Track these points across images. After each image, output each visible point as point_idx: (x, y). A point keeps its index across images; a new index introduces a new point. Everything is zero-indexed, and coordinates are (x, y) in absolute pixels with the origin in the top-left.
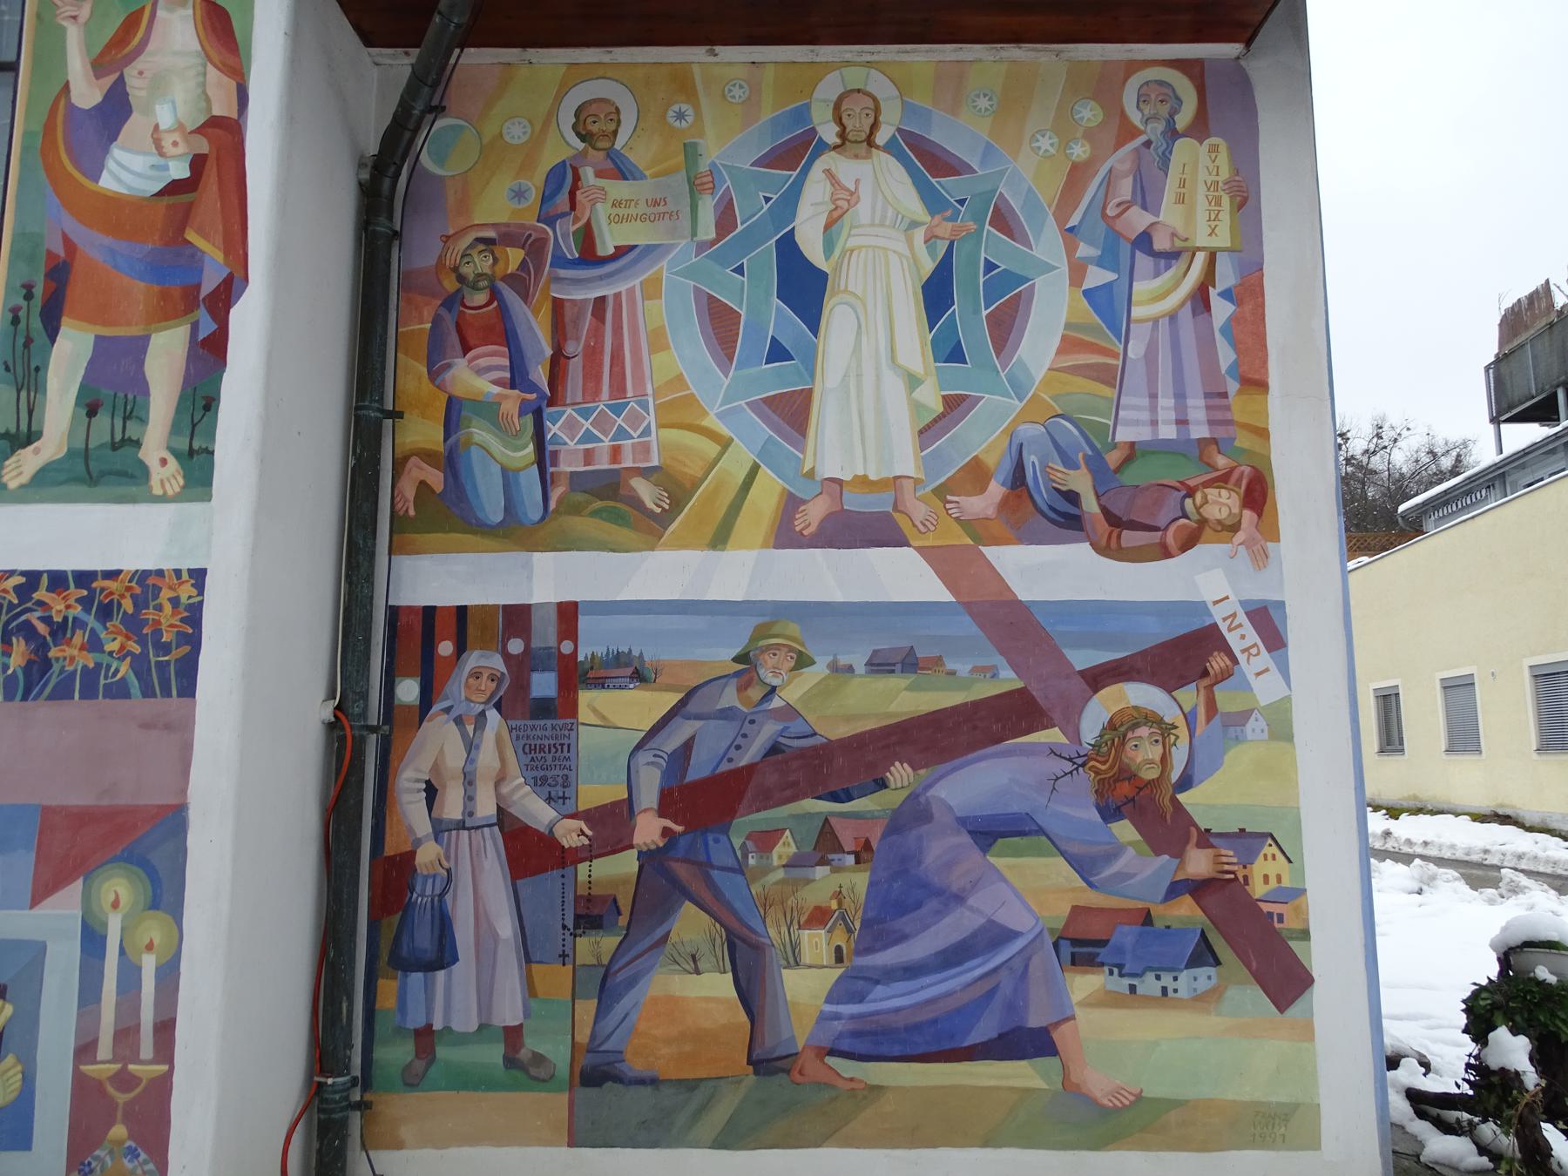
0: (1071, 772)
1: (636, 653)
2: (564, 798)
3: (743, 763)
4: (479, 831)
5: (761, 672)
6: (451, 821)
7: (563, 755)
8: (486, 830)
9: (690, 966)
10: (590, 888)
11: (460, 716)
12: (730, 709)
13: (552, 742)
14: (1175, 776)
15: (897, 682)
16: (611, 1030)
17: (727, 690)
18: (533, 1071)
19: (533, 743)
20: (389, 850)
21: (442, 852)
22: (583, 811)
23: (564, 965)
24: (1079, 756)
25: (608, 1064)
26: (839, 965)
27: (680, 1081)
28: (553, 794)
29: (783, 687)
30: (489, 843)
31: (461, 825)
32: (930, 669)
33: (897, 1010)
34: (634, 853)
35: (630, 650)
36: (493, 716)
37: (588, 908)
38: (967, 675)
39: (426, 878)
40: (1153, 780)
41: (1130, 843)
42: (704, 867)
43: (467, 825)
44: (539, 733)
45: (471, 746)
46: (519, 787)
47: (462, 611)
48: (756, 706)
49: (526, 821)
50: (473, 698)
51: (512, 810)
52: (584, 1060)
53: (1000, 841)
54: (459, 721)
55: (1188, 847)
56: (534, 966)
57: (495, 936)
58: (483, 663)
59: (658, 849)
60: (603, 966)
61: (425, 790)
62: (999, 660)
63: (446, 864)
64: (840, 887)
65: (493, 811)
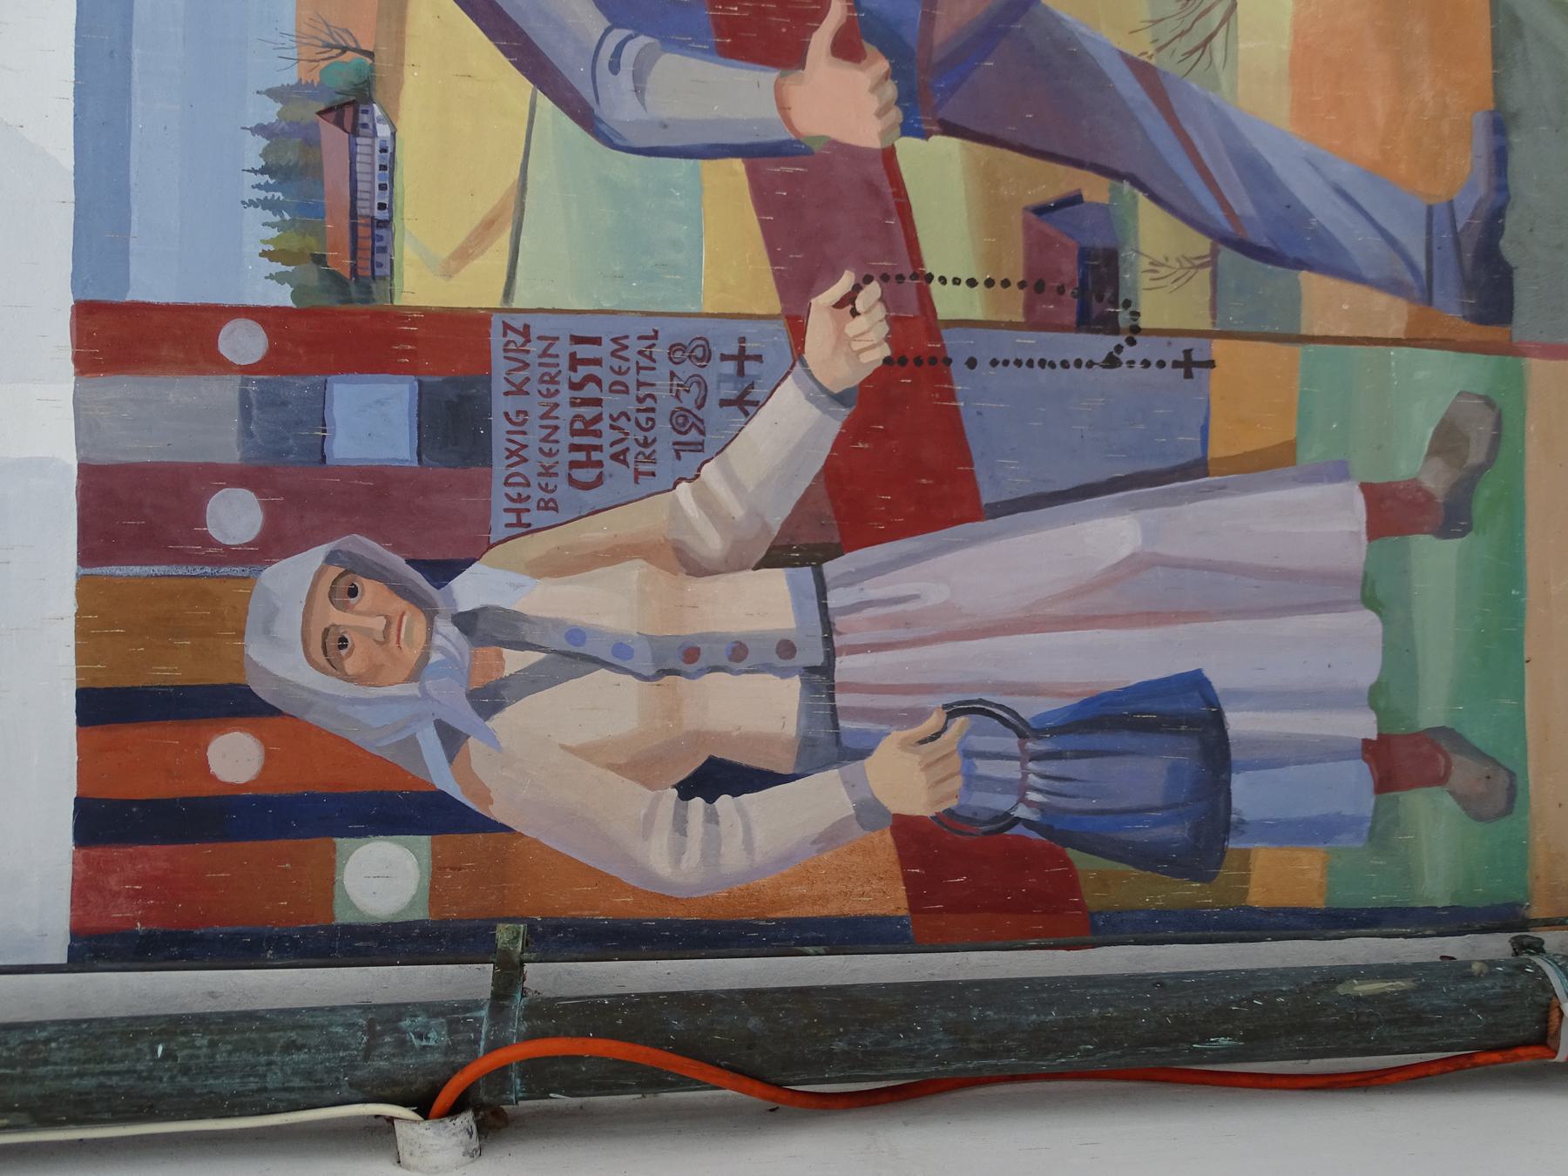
1: (270, 112)
2: (741, 357)
4: (839, 622)
6: (807, 711)
7: (609, 361)
8: (835, 599)
10: (1006, 283)
11: (473, 696)
13: (565, 394)
16: (1375, 240)
18: (1476, 455)
19: (566, 456)
20: (891, 900)
21: (897, 735)
22: (782, 300)
23: (1211, 364)
25: (1457, 242)
27: (1498, 56)
28: (729, 391)
30: (875, 589)
31: (821, 678)
34: (908, 149)
35: (260, 130)
37: (1061, 290)
39: (973, 781)
43: (819, 660)
46: (706, 502)
49: (805, 483)
50: (412, 654)
51: (776, 521)
52: (1450, 309)
54: (489, 700)
56: (1217, 450)
57: (1136, 565)
58: (290, 624)
59: (895, 74)
60: (1214, 253)
61: (710, 799)
63: (933, 723)
65: (777, 580)
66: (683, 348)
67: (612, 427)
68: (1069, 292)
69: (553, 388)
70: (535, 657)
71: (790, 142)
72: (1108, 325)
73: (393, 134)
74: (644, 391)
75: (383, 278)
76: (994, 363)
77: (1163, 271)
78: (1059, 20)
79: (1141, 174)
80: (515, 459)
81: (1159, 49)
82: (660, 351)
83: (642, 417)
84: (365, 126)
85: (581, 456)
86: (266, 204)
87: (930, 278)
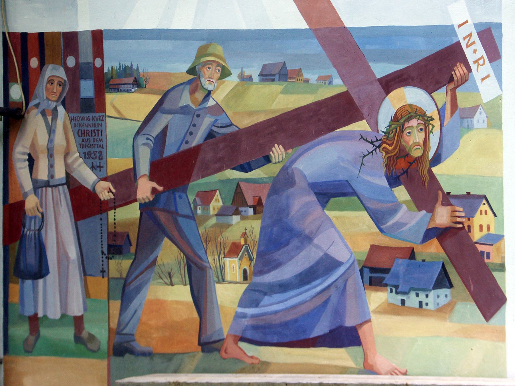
0: (372, 152)
3: (194, 144)
5: (202, 80)
9: (168, 281)
11: (44, 110)
12: (187, 106)
13: (93, 129)
14: (431, 154)
15: (276, 87)
17: (184, 94)
22: (111, 176)
24: (377, 140)
26: (245, 282)
28: (95, 164)
29: (215, 90)
32: (294, 78)
33: (276, 312)
34: (136, 205)
35: (132, 65)
36: (61, 109)
37: (115, 241)
38: (315, 82)
40: (419, 157)
41: (405, 202)
42: (174, 214)
44: (86, 122)
45: (51, 131)
46: (76, 160)
47: (41, 36)
48: (200, 105)
50: (50, 98)
53: (332, 200)
55: (437, 205)
59: (150, 201)
62: (333, 72)
64: (246, 230)
66: (101, 154)
67: (88, 139)
68: (114, 243)
69: (94, 126)
70: (50, 124)
71: (137, 178)
72: (109, 253)
73: (133, 92)
74: (94, 145)
75: (110, 91)
76: (101, 225)
77: (119, 265)
78: (162, 241)
79: (136, 261)
80: (82, 118)
81: (159, 266)
82: (100, 149)
83: (89, 145)
84: (134, 86)
85: (83, 132)
86: (120, 66)
87: (115, 210)
